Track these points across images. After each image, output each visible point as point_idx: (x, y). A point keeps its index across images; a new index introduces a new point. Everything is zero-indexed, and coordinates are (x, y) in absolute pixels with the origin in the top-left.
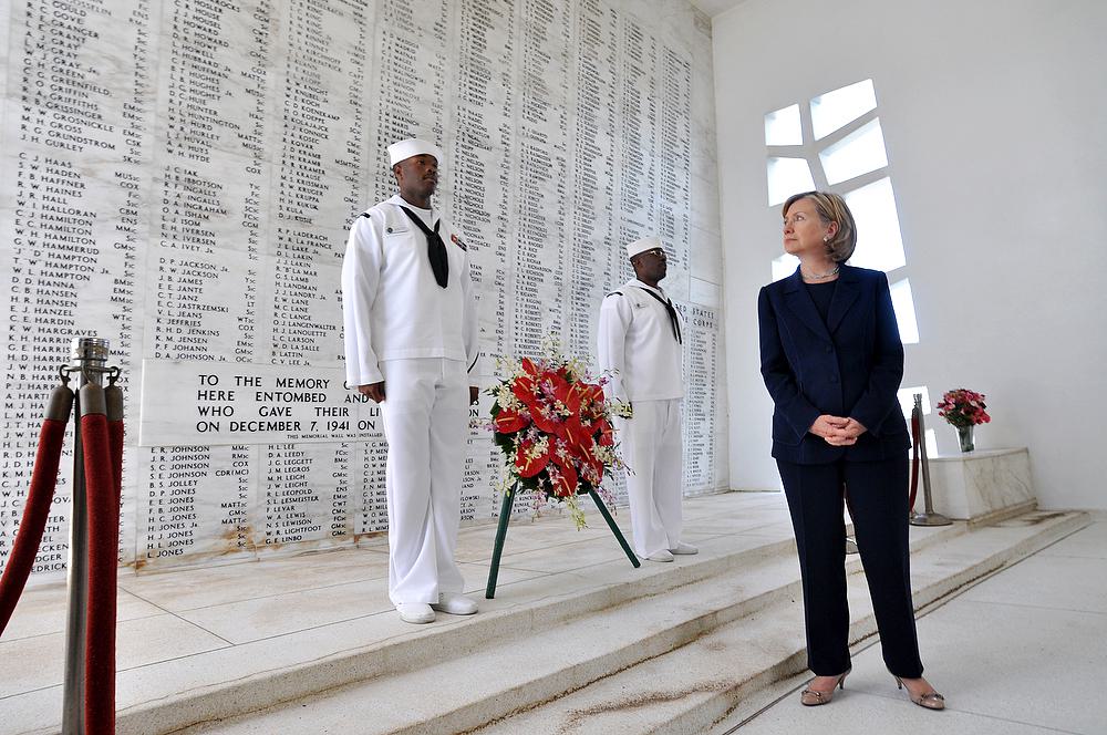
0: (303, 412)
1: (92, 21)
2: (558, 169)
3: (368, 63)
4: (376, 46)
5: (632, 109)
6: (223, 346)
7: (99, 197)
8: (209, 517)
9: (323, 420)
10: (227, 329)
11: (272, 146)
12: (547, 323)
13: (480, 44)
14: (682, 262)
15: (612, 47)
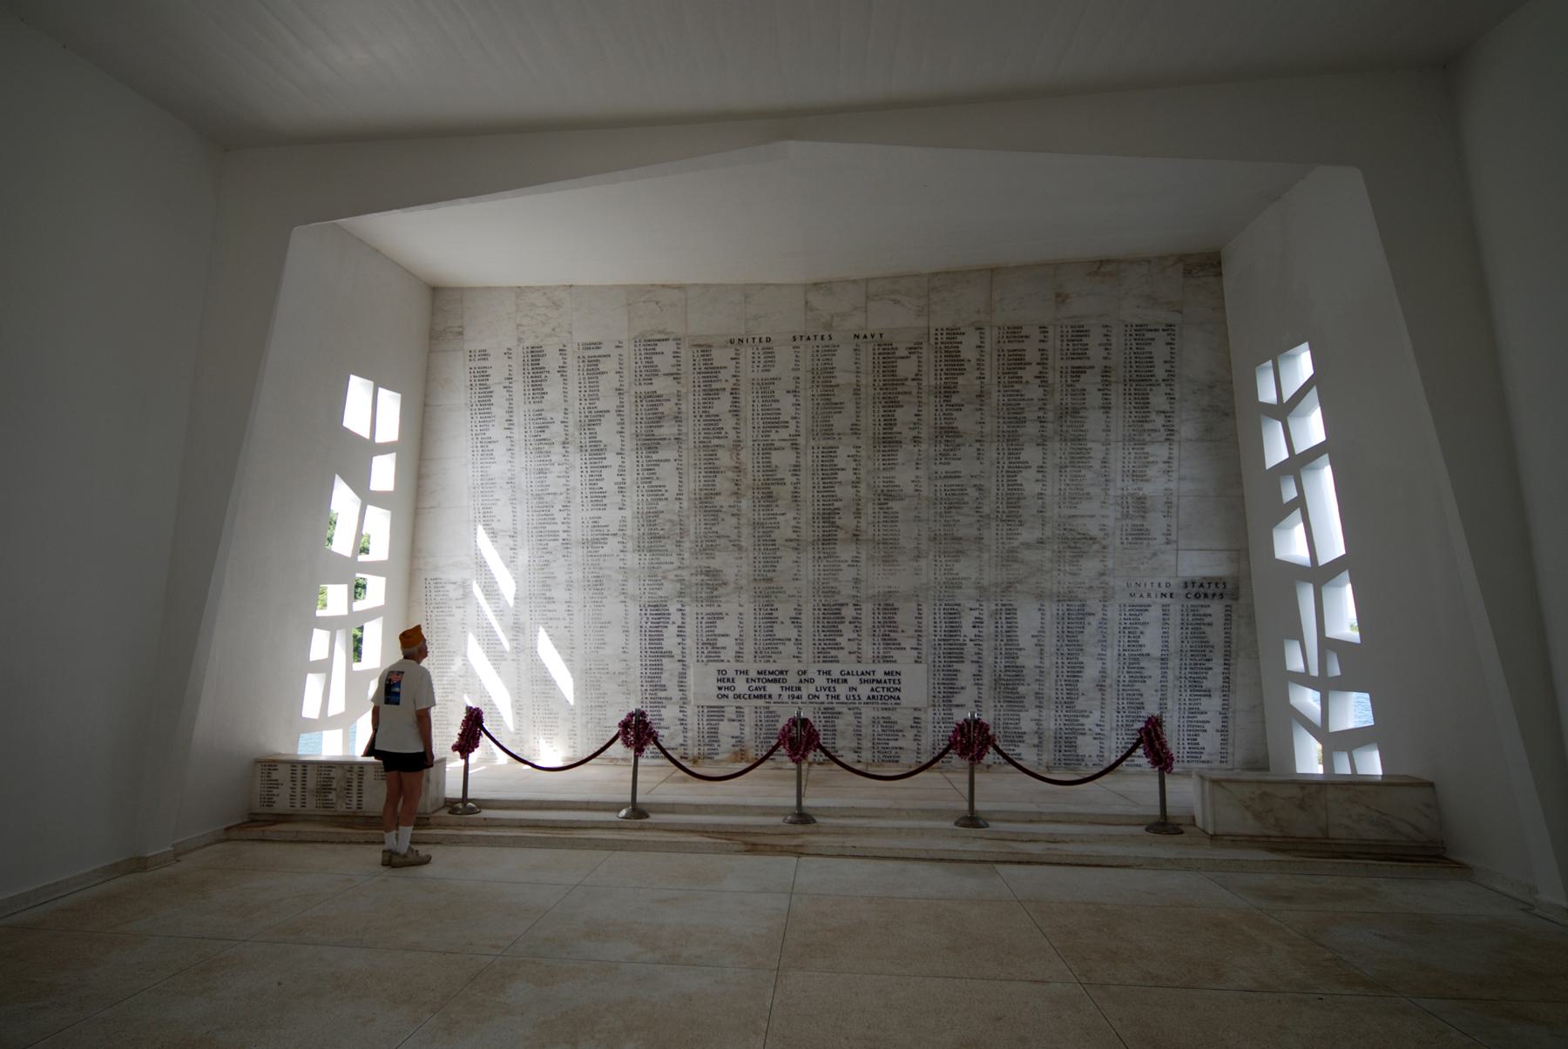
0: (774, 689)
1: (661, 506)
2: (973, 493)
3: (803, 474)
4: (807, 460)
5: (1072, 412)
6: (728, 654)
7: (669, 588)
8: (726, 745)
9: (785, 694)
10: (729, 644)
11: (746, 542)
12: (967, 621)
13: (890, 423)
14: (1162, 539)
15: (1043, 363)
